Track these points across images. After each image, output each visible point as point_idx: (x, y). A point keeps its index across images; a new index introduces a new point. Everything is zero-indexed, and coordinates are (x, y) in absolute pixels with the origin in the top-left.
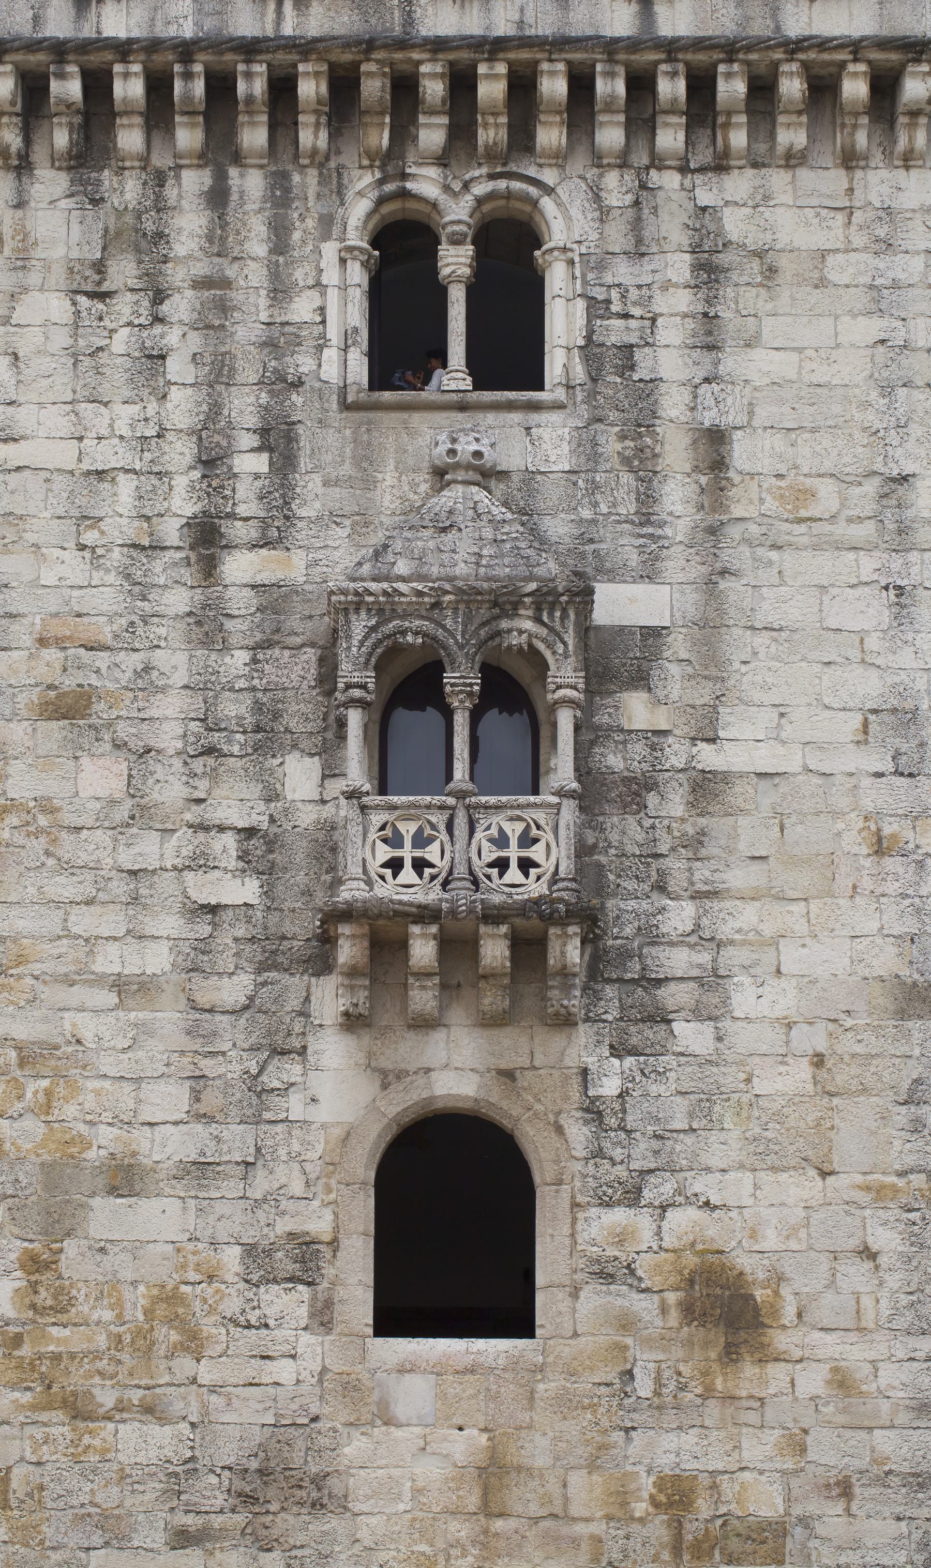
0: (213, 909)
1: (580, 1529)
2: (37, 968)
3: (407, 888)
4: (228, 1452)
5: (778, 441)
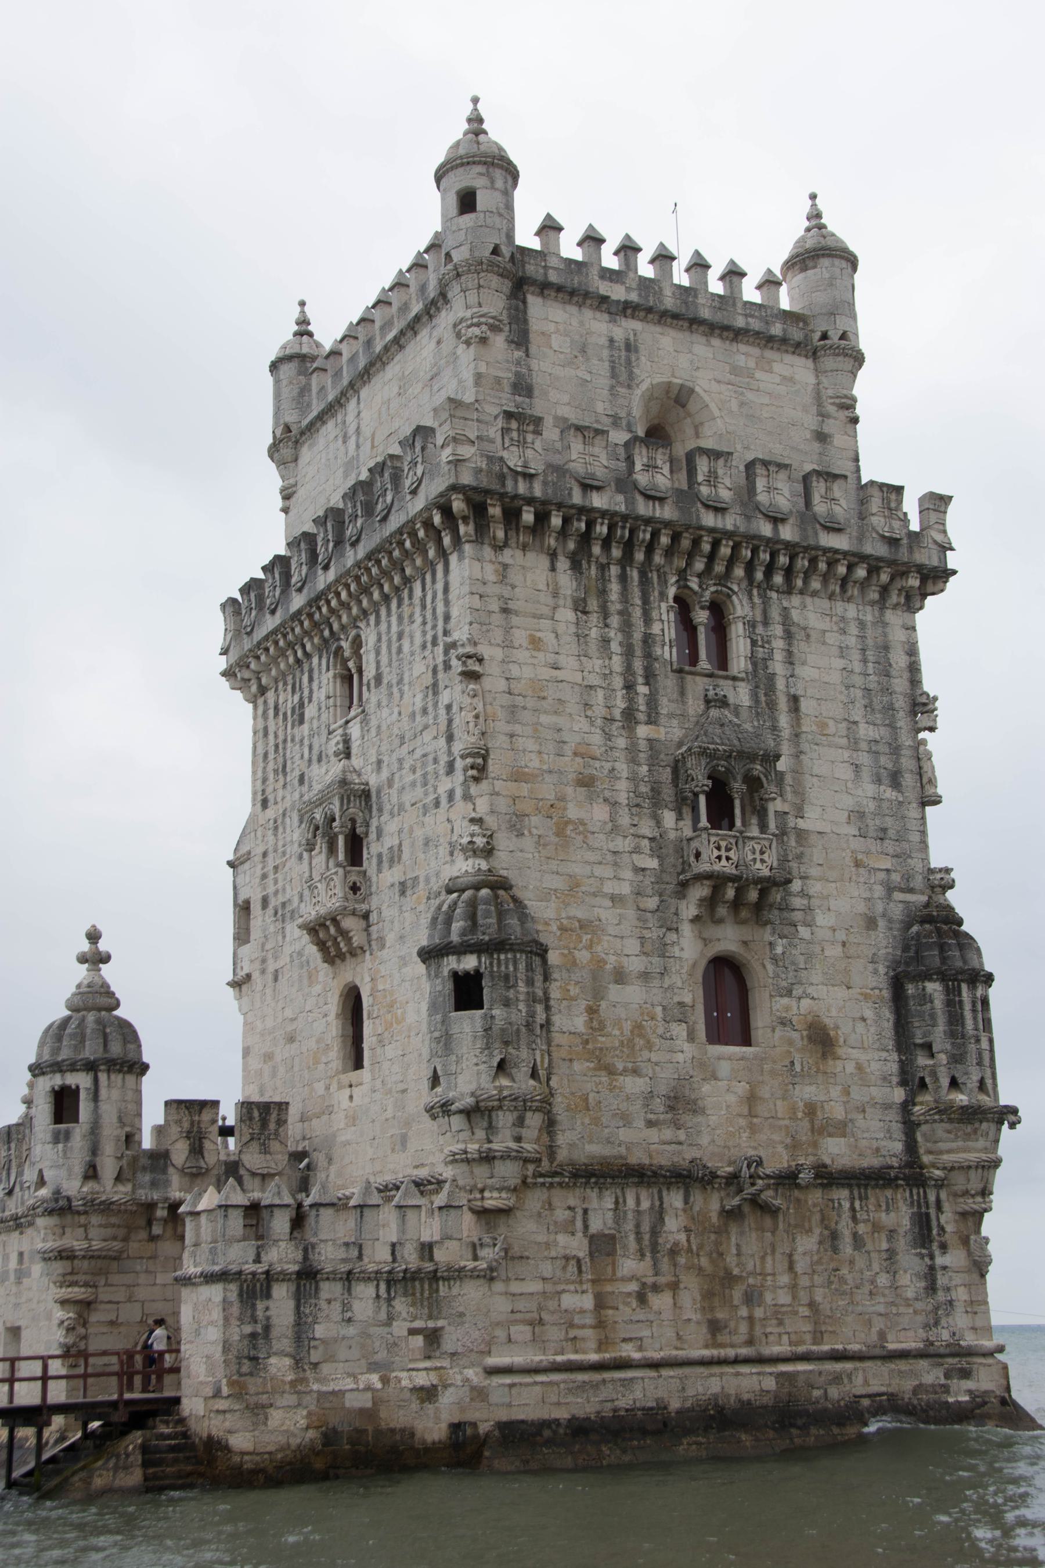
0: (643, 870)
1: (782, 1123)
2: (584, 889)
3: (724, 867)
4: (663, 1089)
5: (813, 703)
